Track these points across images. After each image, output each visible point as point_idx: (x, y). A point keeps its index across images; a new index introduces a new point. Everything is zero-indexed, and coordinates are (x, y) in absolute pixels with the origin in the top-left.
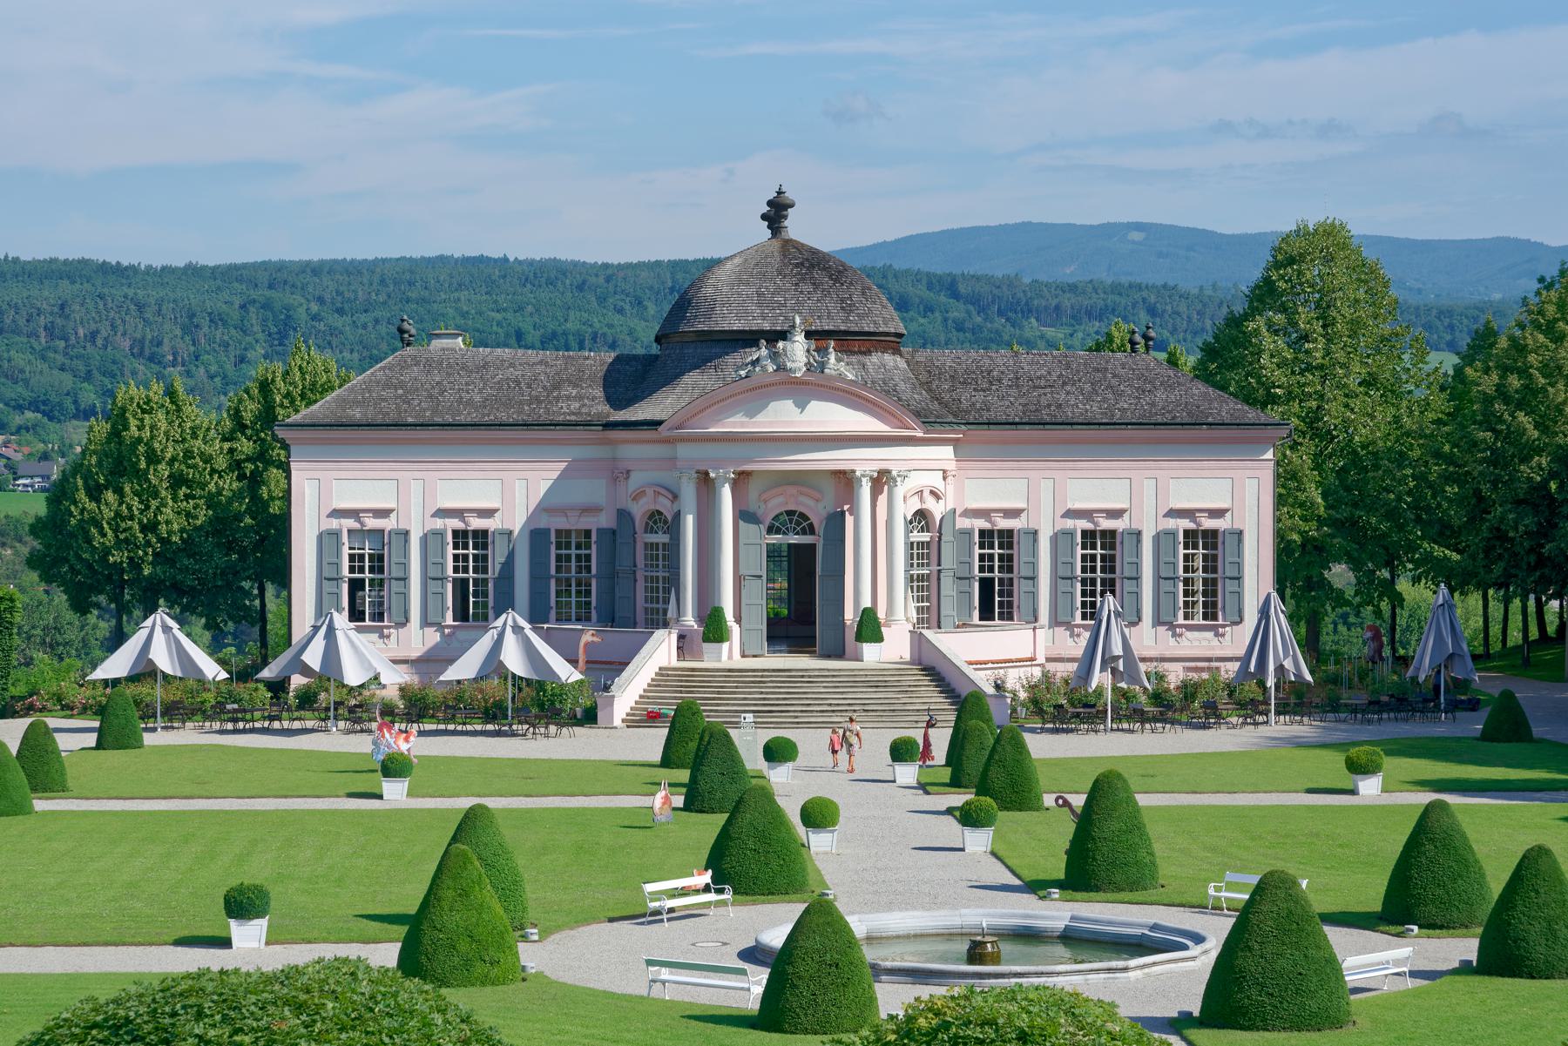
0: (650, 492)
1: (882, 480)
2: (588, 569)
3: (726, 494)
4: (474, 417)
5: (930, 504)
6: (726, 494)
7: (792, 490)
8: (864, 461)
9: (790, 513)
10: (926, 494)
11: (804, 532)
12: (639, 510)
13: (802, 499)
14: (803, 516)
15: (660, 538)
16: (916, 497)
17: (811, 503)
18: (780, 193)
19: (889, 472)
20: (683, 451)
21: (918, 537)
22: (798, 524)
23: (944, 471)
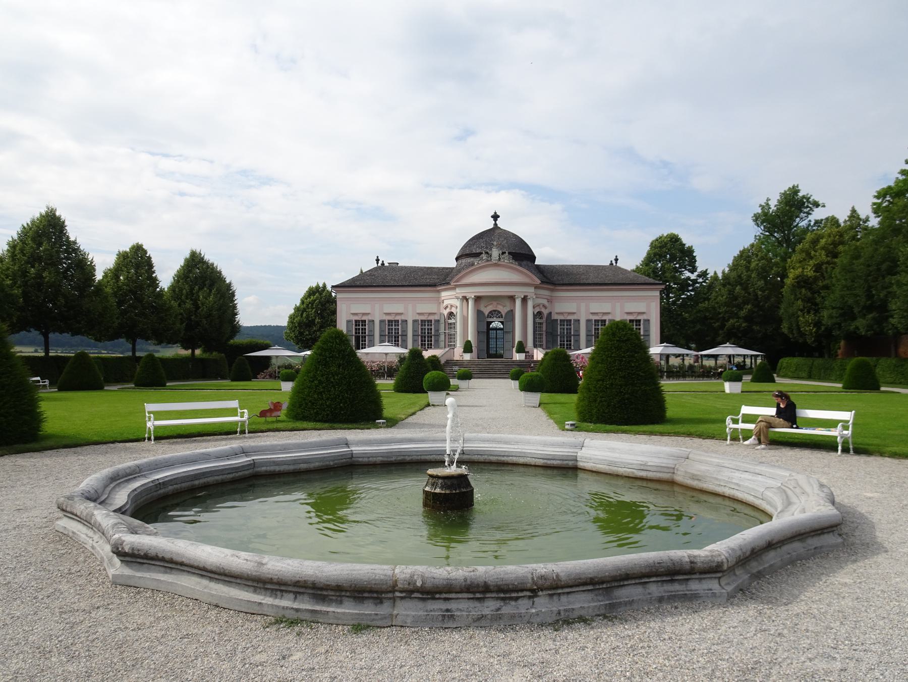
0: (449, 307)
1: (525, 300)
2: (431, 333)
3: (471, 302)
4: (396, 284)
5: (543, 310)
6: (471, 302)
7: (495, 303)
8: (519, 292)
9: (495, 311)
10: (541, 306)
11: (499, 317)
12: (446, 312)
13: (499, 306)
14: (499, 312)
15: (452, 321)
16: (538, 307)
17: (502, 307)
18: (495, 213)
19: (527, 296)
20: (458, 290)
21: (538, 320)
22: (497, 315)
23: (548, 299)
